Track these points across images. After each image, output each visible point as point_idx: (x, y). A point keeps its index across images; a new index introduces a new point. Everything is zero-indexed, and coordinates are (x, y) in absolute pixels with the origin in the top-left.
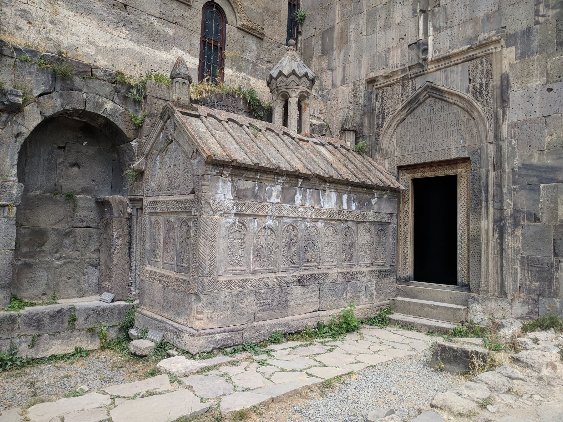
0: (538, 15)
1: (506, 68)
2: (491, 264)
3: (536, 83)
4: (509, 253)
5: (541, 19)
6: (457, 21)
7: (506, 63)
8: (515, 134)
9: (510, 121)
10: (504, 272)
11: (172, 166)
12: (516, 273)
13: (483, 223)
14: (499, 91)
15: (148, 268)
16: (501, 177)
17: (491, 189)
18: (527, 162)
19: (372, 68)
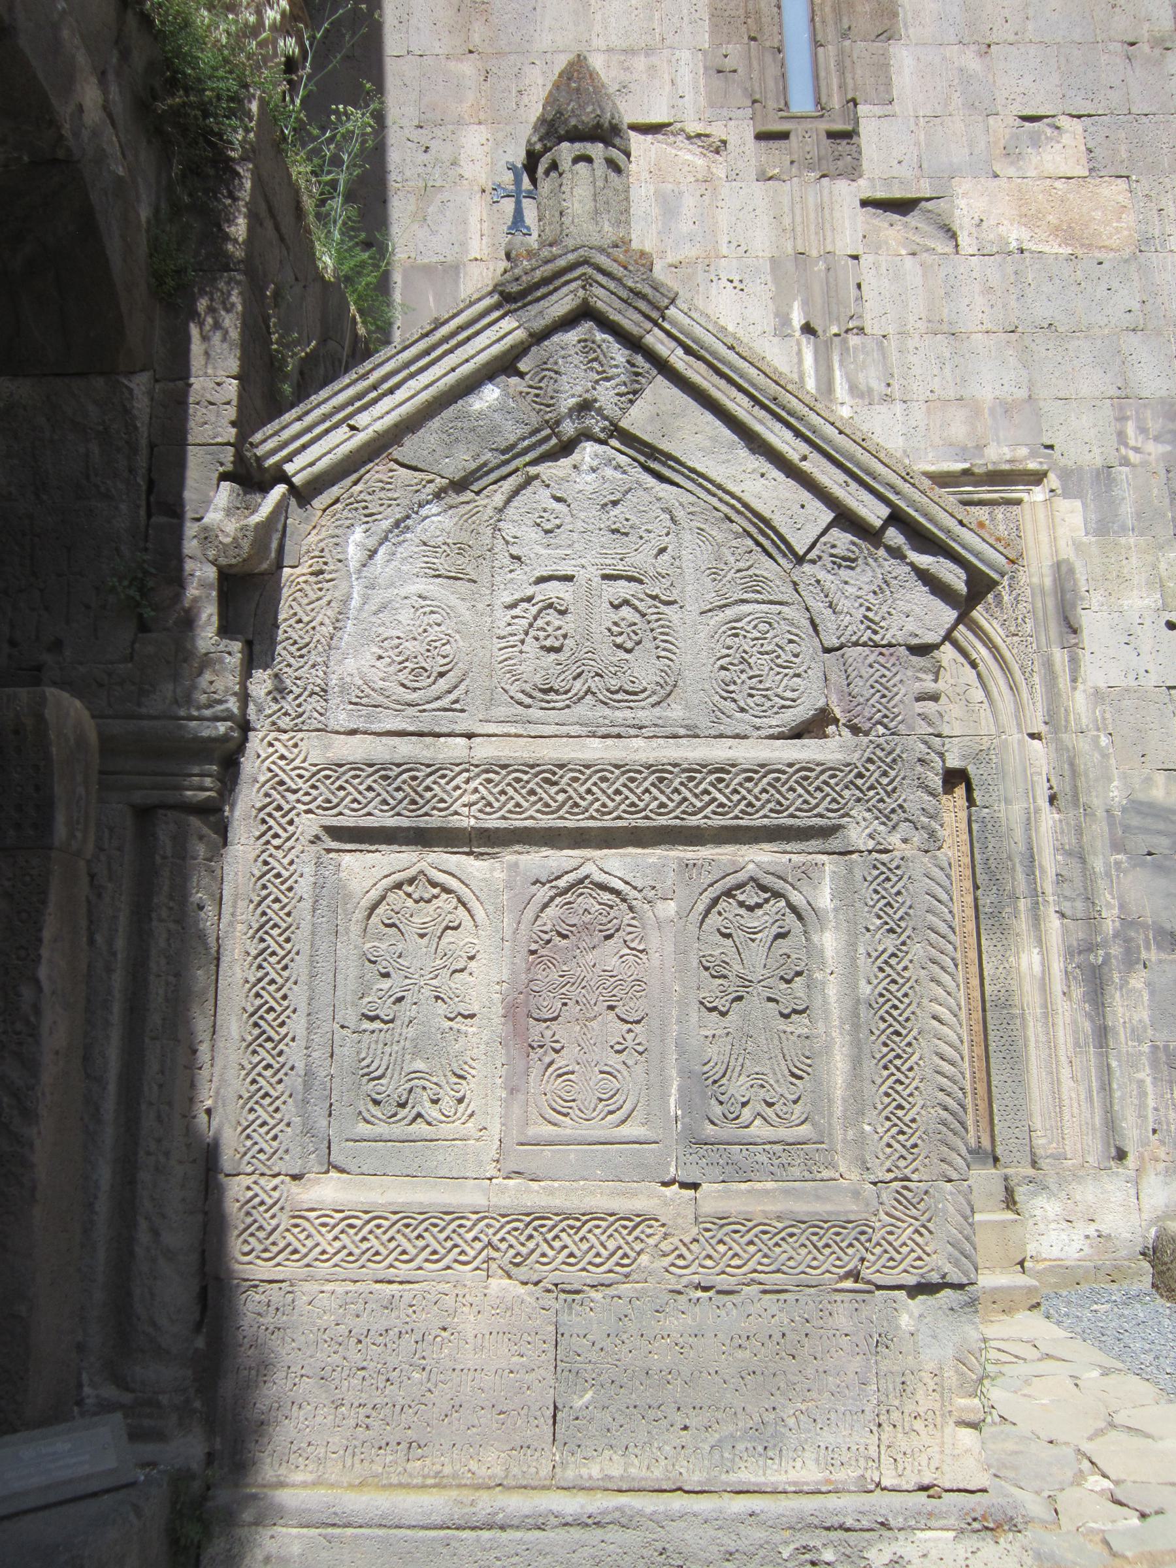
0: (1126, 445)
1: (1067, 552)
2: (1065, 1072)
3: (1139, 603)
5: (1132, 456)
8: (1104, 719)
9: (1090, 684)
10: (1117, 1094)
11: (588, 574)
12: (1143, 1094)
13: (1024, 958)
14: (1050, 603)
15: (326, 1191)
16: (1079, 831)
17: (1049, 862)
18: (1141, 796)
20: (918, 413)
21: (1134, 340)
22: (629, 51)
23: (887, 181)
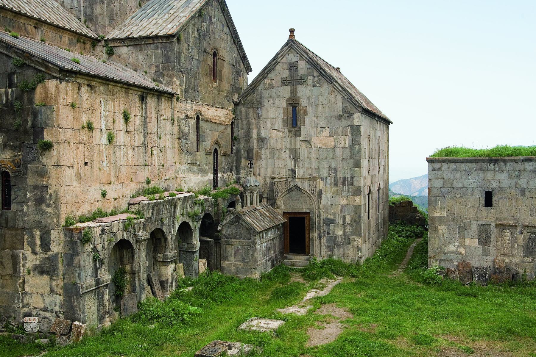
4: (322, 244)
6: (306, 166)
7: (321, 186)
15: (226, 262)
17: (317, 223)
19: (273, 173)
20: (305, 169)
21: (332, 160)
22: (273, 119)
23: (304, 138)
